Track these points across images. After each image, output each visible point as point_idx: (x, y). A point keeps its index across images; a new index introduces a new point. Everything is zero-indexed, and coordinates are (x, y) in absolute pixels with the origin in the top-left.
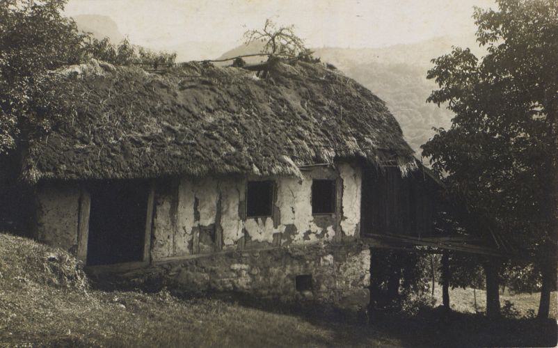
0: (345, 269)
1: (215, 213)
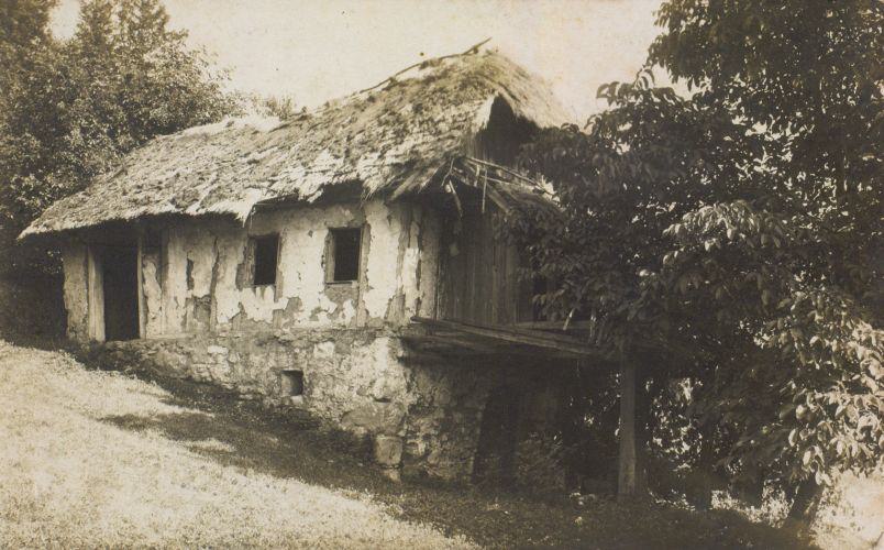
0: (349, 367)
1: (209, 280)
